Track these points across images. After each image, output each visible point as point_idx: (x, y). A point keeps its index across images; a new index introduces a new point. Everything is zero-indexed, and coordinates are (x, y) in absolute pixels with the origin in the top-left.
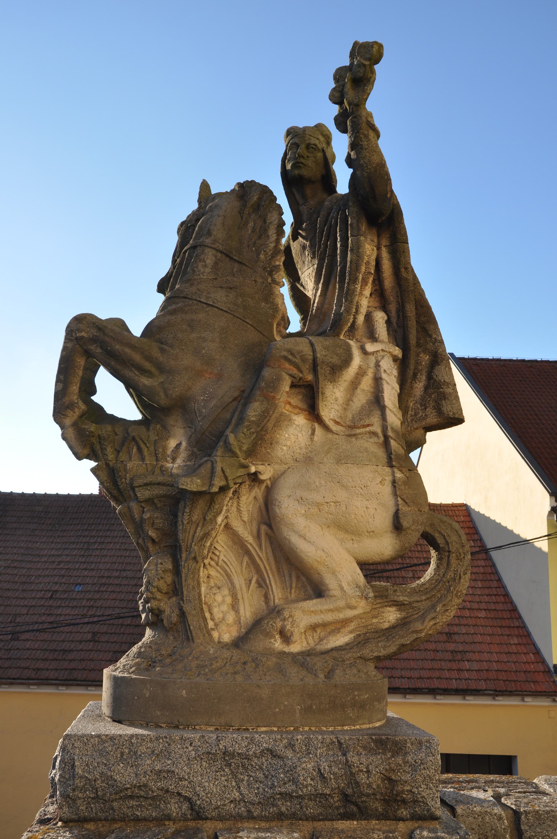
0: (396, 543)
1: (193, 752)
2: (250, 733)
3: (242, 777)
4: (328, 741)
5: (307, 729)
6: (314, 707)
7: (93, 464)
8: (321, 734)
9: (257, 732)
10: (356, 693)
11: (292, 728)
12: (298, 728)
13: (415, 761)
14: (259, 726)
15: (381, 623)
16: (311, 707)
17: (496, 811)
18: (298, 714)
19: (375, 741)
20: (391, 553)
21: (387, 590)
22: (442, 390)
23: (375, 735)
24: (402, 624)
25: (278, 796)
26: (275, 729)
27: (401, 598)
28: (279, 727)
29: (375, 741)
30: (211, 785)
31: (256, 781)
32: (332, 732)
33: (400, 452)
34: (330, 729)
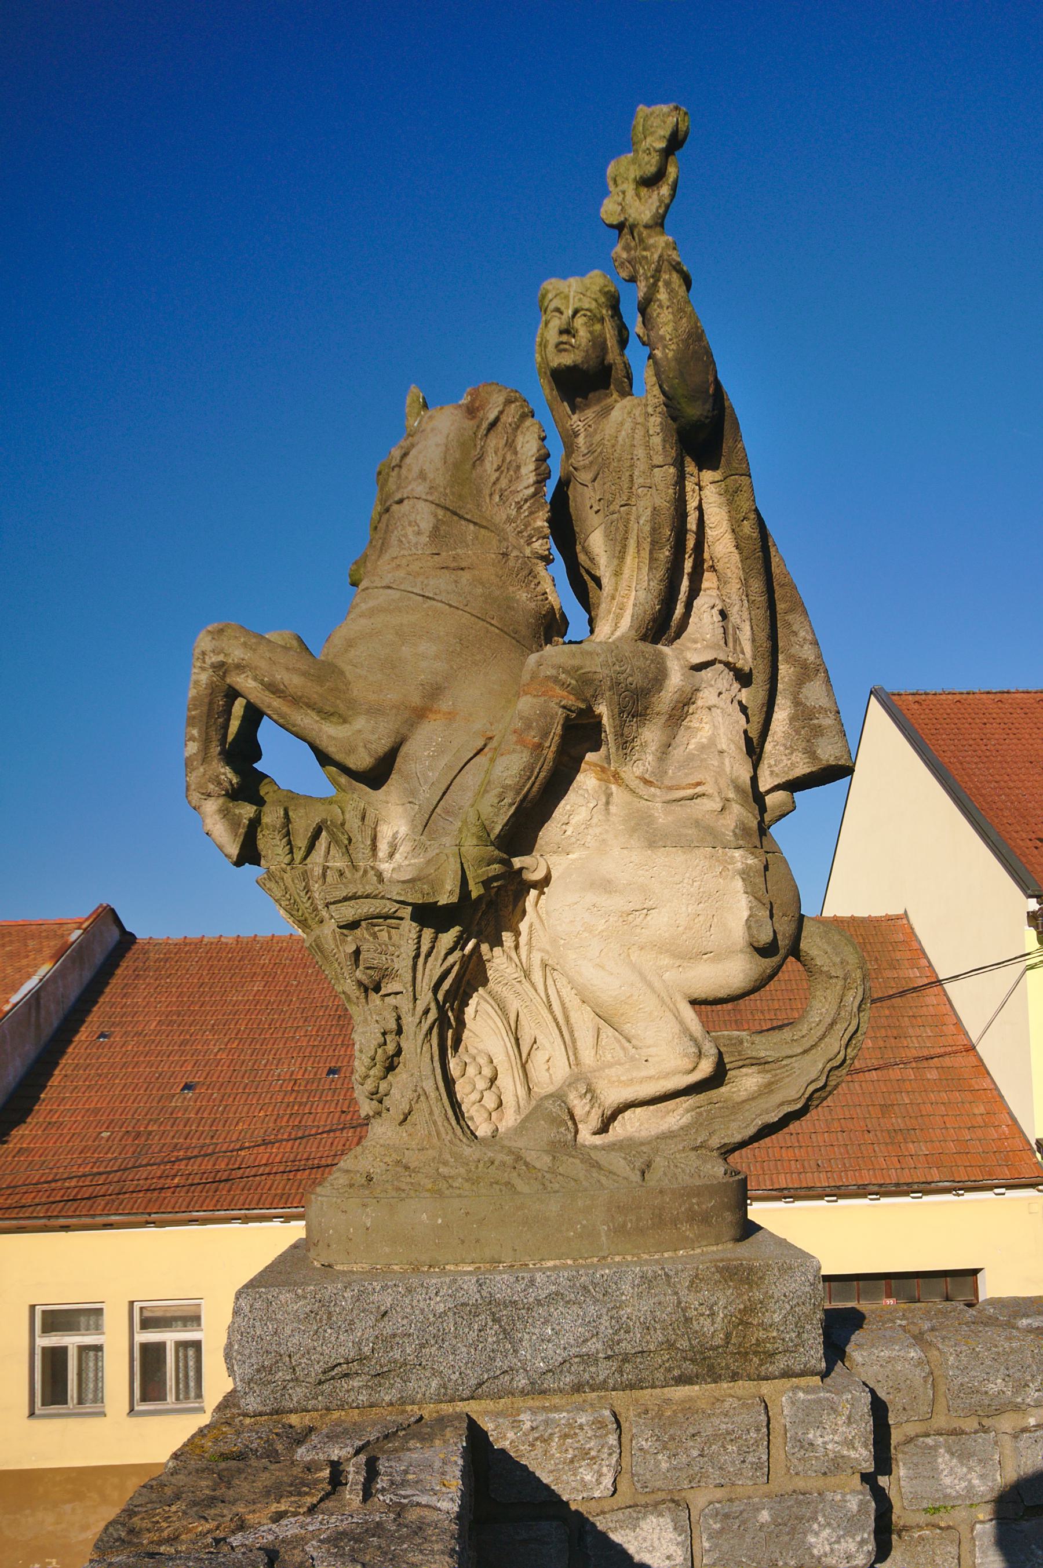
0: (751, 969)
1: (442, 1305)
2: (530, 1271)
3: (520, 1335)
4: (650, 1274)
5: (617, 1259)
6: (629, 1225)
7: (1033, 905)
8: (641, 1265)
9: (540, 1269)
10: (694, 1201)
11: (596, 1259)
12: (604, 1258)
13: (785, 1296)
14: (543, 1260)
15: (733, 1093)
16: (624, 1225)
17: (912, 1354)
18: (604, 1238)
19: (719, 1270)
20: (743, 984)
21: (741, 1042)
22: (816, 721)
23: (722, 1260)
24: (768, 1089)
25: (577, 1360)
26: (570, 1262)
27: (762, 1054)
28: (575, 1260)
29: (719, 1270)
30: (472, 1351)
31: (543, 1340)
32: (657, 1261)
33: (750, 825)
34: (656, 1257)
